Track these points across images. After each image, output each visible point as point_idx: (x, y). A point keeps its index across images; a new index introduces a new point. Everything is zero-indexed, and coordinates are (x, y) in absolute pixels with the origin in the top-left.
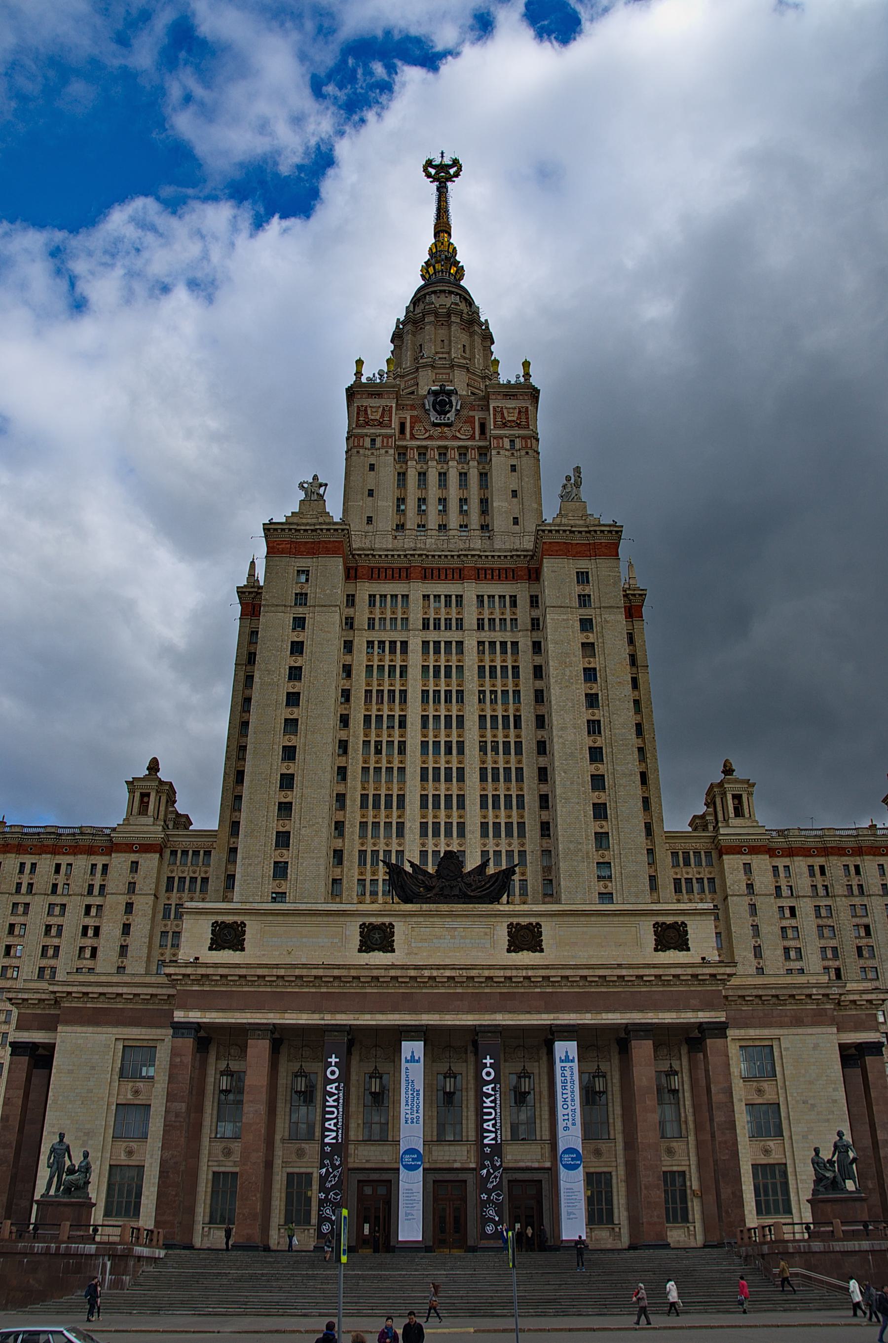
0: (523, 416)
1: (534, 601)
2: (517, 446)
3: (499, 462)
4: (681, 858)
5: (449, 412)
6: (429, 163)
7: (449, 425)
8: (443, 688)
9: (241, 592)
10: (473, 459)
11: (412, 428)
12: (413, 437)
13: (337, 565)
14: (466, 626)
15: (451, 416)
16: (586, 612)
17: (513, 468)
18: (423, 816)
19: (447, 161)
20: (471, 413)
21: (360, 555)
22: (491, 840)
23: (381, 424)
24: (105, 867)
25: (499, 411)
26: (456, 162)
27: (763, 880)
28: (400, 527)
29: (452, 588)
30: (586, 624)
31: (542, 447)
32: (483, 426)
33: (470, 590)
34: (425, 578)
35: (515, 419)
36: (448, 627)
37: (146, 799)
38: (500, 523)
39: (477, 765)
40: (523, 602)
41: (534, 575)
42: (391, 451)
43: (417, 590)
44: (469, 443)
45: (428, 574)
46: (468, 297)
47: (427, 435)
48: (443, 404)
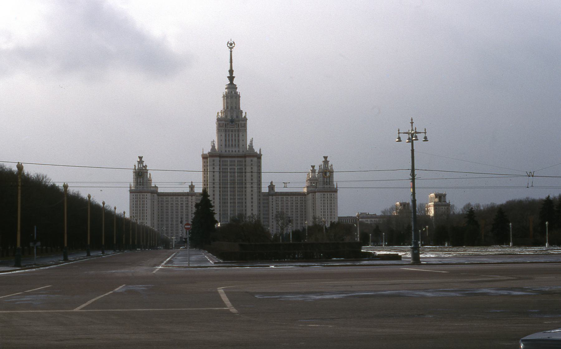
1: (245, 161)
2: (244, 131)
3: (241, 134)
6: (228, 42)
12: (227, 128)
15: (234, 123)
16: (252, 166)
19: (232, 43)
20: (237, 122)
25: (241, 124)
26: (234, 42)
27: (274, 200)
28: (226, 145)
29: (233, 159)
31: (248, 130)
32: (238, 125)
33: (236, 159)
38: (241, 146)
43: (228, 159)
44: (237, 129)
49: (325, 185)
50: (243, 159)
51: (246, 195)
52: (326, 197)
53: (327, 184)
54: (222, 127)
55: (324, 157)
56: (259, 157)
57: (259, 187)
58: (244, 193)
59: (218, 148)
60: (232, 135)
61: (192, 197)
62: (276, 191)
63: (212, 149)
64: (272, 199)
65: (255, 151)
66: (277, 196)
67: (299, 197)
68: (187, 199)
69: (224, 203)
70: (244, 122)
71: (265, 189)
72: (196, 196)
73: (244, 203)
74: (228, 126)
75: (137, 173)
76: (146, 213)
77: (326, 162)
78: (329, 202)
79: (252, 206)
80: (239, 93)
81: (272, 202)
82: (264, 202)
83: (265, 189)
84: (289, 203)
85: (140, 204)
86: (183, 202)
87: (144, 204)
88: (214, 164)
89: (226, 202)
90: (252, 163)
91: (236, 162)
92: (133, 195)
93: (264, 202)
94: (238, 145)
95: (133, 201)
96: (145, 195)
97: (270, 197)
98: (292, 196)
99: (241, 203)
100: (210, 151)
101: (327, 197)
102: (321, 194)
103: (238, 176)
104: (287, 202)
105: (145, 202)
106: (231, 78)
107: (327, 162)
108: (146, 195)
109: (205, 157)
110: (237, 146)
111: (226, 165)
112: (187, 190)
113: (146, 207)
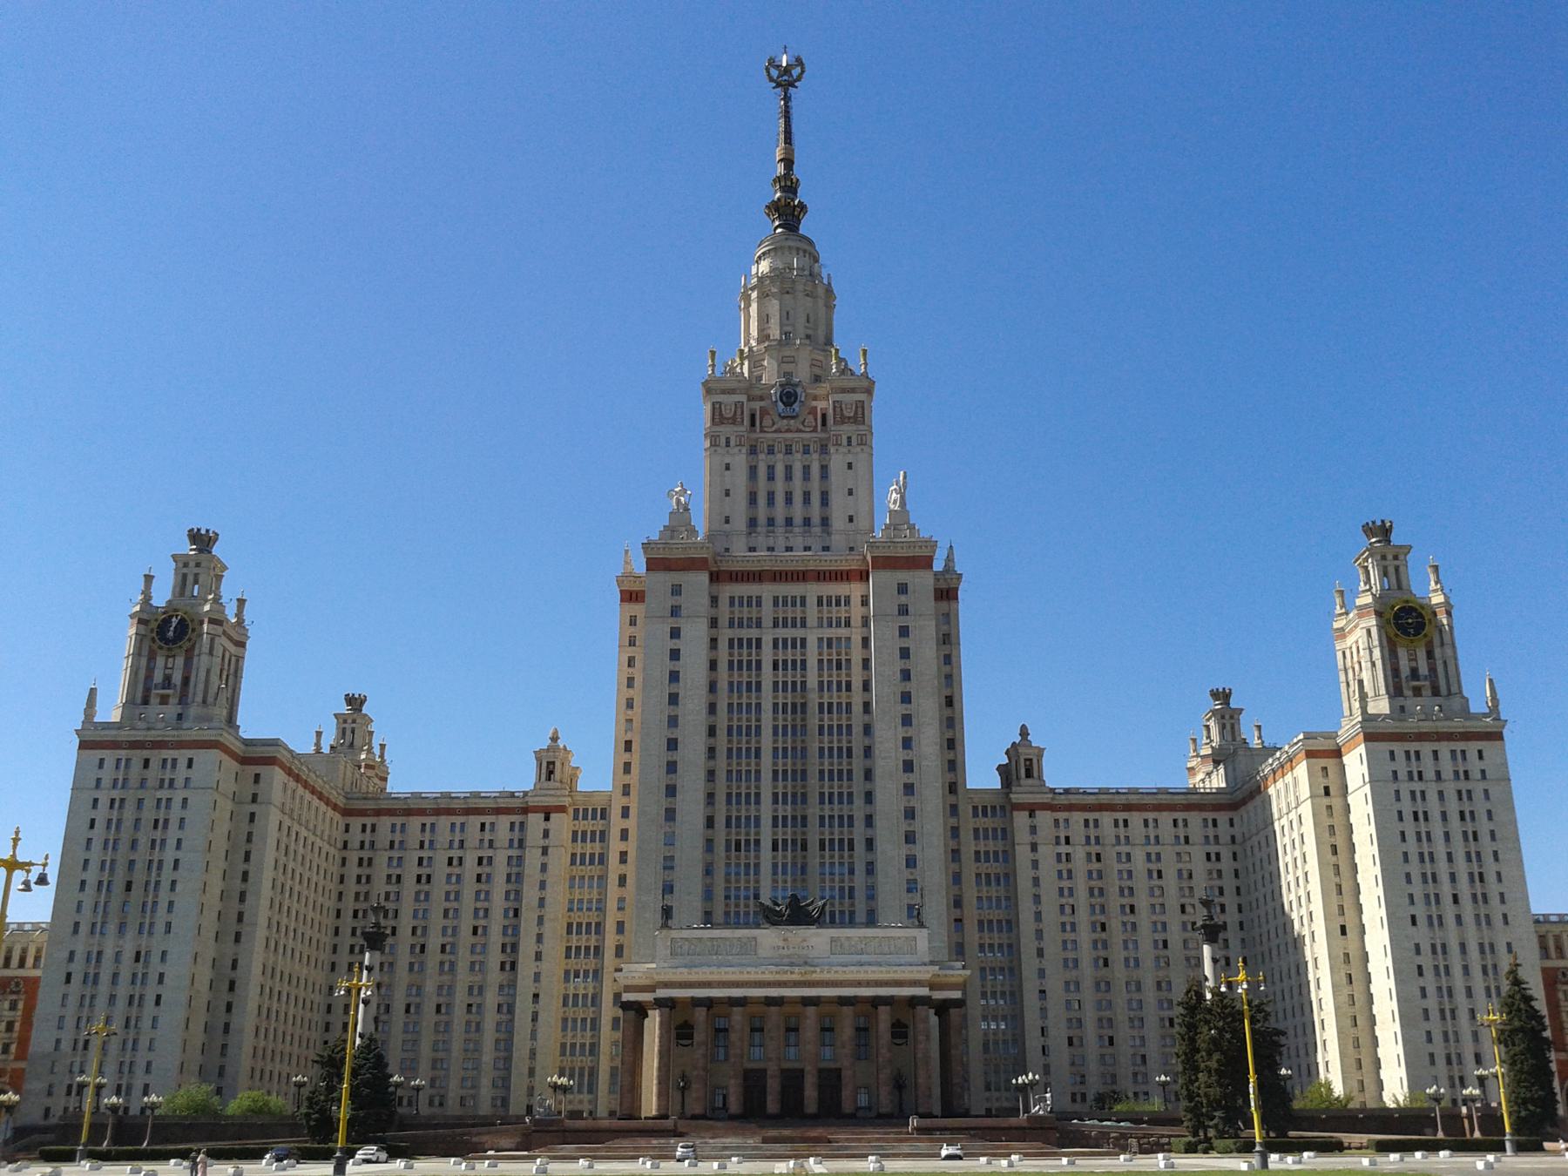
0: (860, 410)
1: (865, 602)
3: (837, 461)
4: (981, 810)
5: (795, 401)
7: (793, 418)
8: (790, 680)
9: (620, 581)
10: (815, 452)
11: (761, 423)
12: (762, 431)
13: (704, 577)
14: (809, 624)
15: (796, 406)
17: (850, 466)
18: (775, 787)
20: (814, 403)
21: (721, 561)
22: (827, 806)
23: (734, 423)
24: (522, 824)
26: (799, 62)
28: (752, 522)
30: (904, 632)
31: (877, 441)
32: (824, 416)
33: (812, 590)
34: (775, 580)
35: (852, 415)
36: (794, 625)
37: (551, 766)
38: (838, 522)
39: (817, 745)
40: (856, 600)
41: (863, 576)
42: (744, 450)
44: (814, 435)
45: (778, 576)
46: (813, 251)
47: (774, 429)
48: (789, 395)
49: (1408, 693)
50: (854, 590)
51: (869, 797)
52: (1429, 774)
53: (1417, 692)
54: (733, 421)
55: (1369, 530)
56: (947, 594)
57: (954, 766)
58: (858, 785)
59: (711, 536)
60: (789, 469)
61: (547, 819)
62: (1050, 784)
63: (670, 530)
64: (1033, 830)
65: (925, 534)
66: (1061, 816)
67: (1195, 818)
68: (516, 835)
69: (738, 849)
70: (862, 397)
71: (982, 775)
72: (576, 818)
73: (860, 847)
74: (767, 421)
75: (154, 625)
76: (174, 883)
77: (1390, 557)
78: (1453, 807)
79: (911, 862)
80: (829, 275)
81: (1034, 847)
82: (982, 849)
83: (982, 775)
84: (1139, 855)
85: (138, 820)
86: (490, 853)
87: (166, 821)
88: (675, 611)
89: (748, 842)
90: (903, 599)
91: (812, 601)
92: (102, 761)
93: (982, 849)
94: (825, 522)
95: (96, 801)
96: (182, 764)
97: (1021, 818)
98: (1150, 816)
99: (841, 849)
100: (655, 537)
101: (1438, 774)
102: (1392, 753)
103: (821, 683)
104: (1124, 849)
105: (176, 812)
106: (788, 213)
107: (1396, 558)
108: (190, 763)
109: (631, 596)
110: (816, 520)
111: (750, 619)
112: (522, 779)
113: (178, 846)
